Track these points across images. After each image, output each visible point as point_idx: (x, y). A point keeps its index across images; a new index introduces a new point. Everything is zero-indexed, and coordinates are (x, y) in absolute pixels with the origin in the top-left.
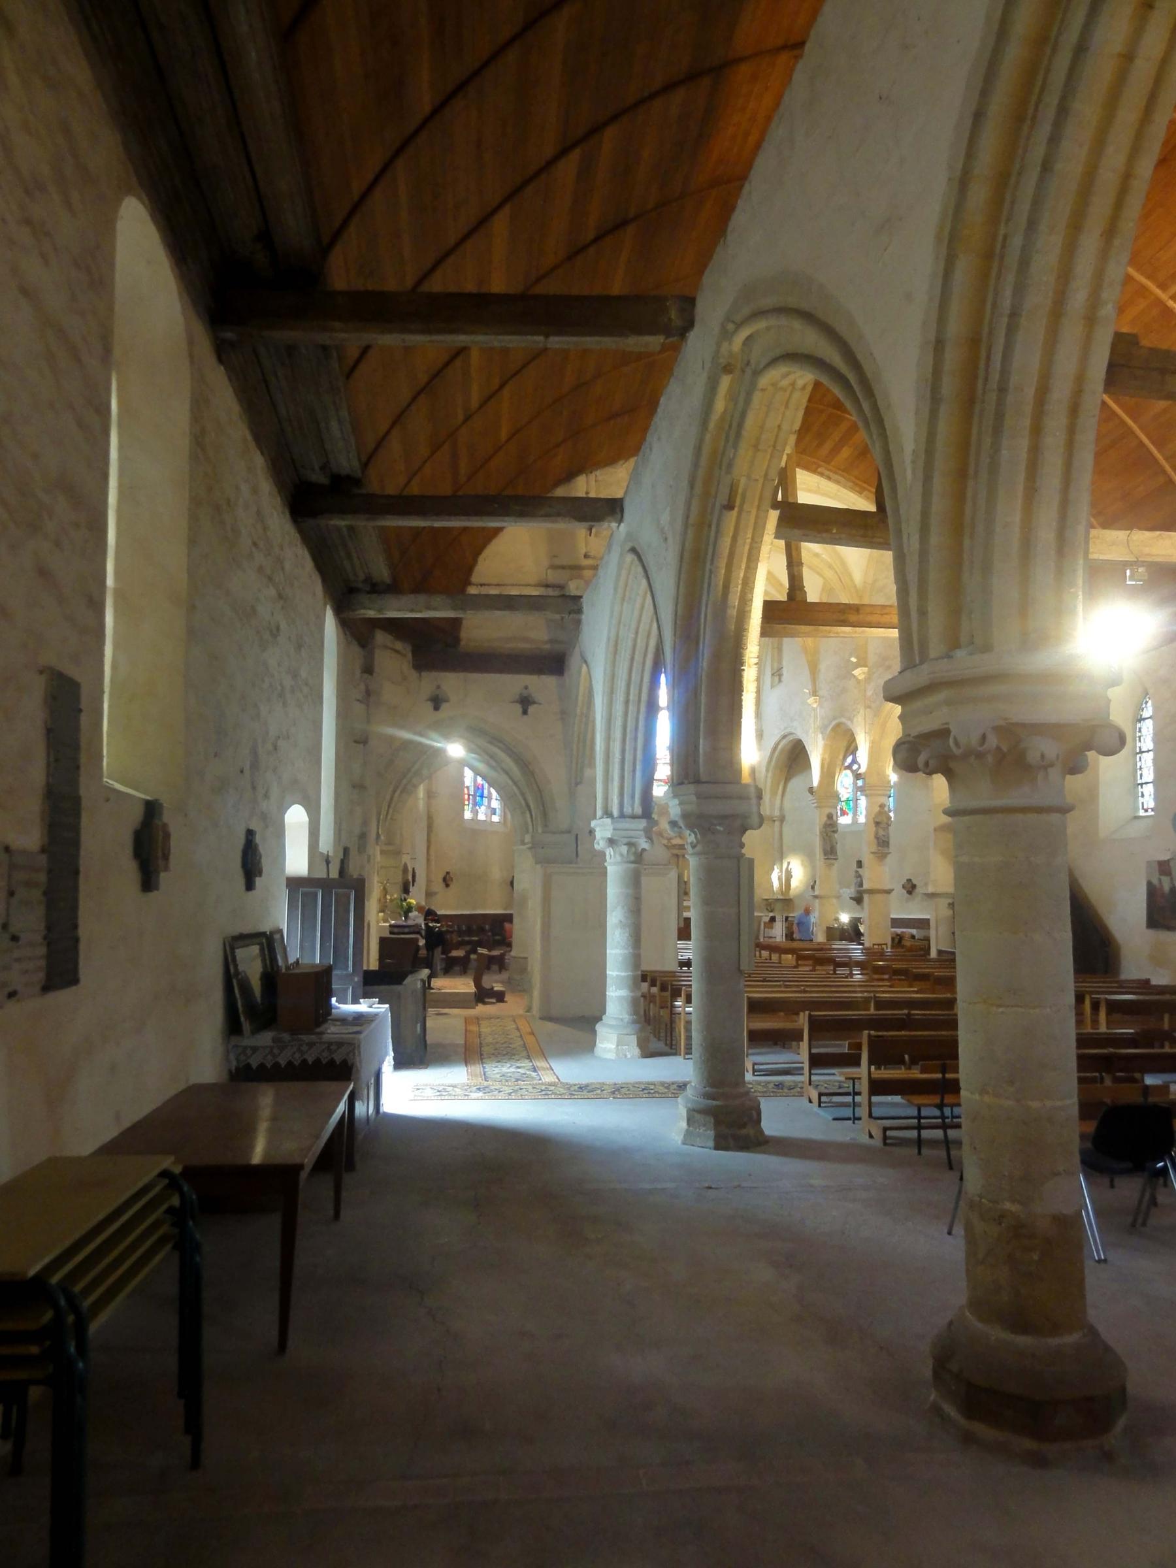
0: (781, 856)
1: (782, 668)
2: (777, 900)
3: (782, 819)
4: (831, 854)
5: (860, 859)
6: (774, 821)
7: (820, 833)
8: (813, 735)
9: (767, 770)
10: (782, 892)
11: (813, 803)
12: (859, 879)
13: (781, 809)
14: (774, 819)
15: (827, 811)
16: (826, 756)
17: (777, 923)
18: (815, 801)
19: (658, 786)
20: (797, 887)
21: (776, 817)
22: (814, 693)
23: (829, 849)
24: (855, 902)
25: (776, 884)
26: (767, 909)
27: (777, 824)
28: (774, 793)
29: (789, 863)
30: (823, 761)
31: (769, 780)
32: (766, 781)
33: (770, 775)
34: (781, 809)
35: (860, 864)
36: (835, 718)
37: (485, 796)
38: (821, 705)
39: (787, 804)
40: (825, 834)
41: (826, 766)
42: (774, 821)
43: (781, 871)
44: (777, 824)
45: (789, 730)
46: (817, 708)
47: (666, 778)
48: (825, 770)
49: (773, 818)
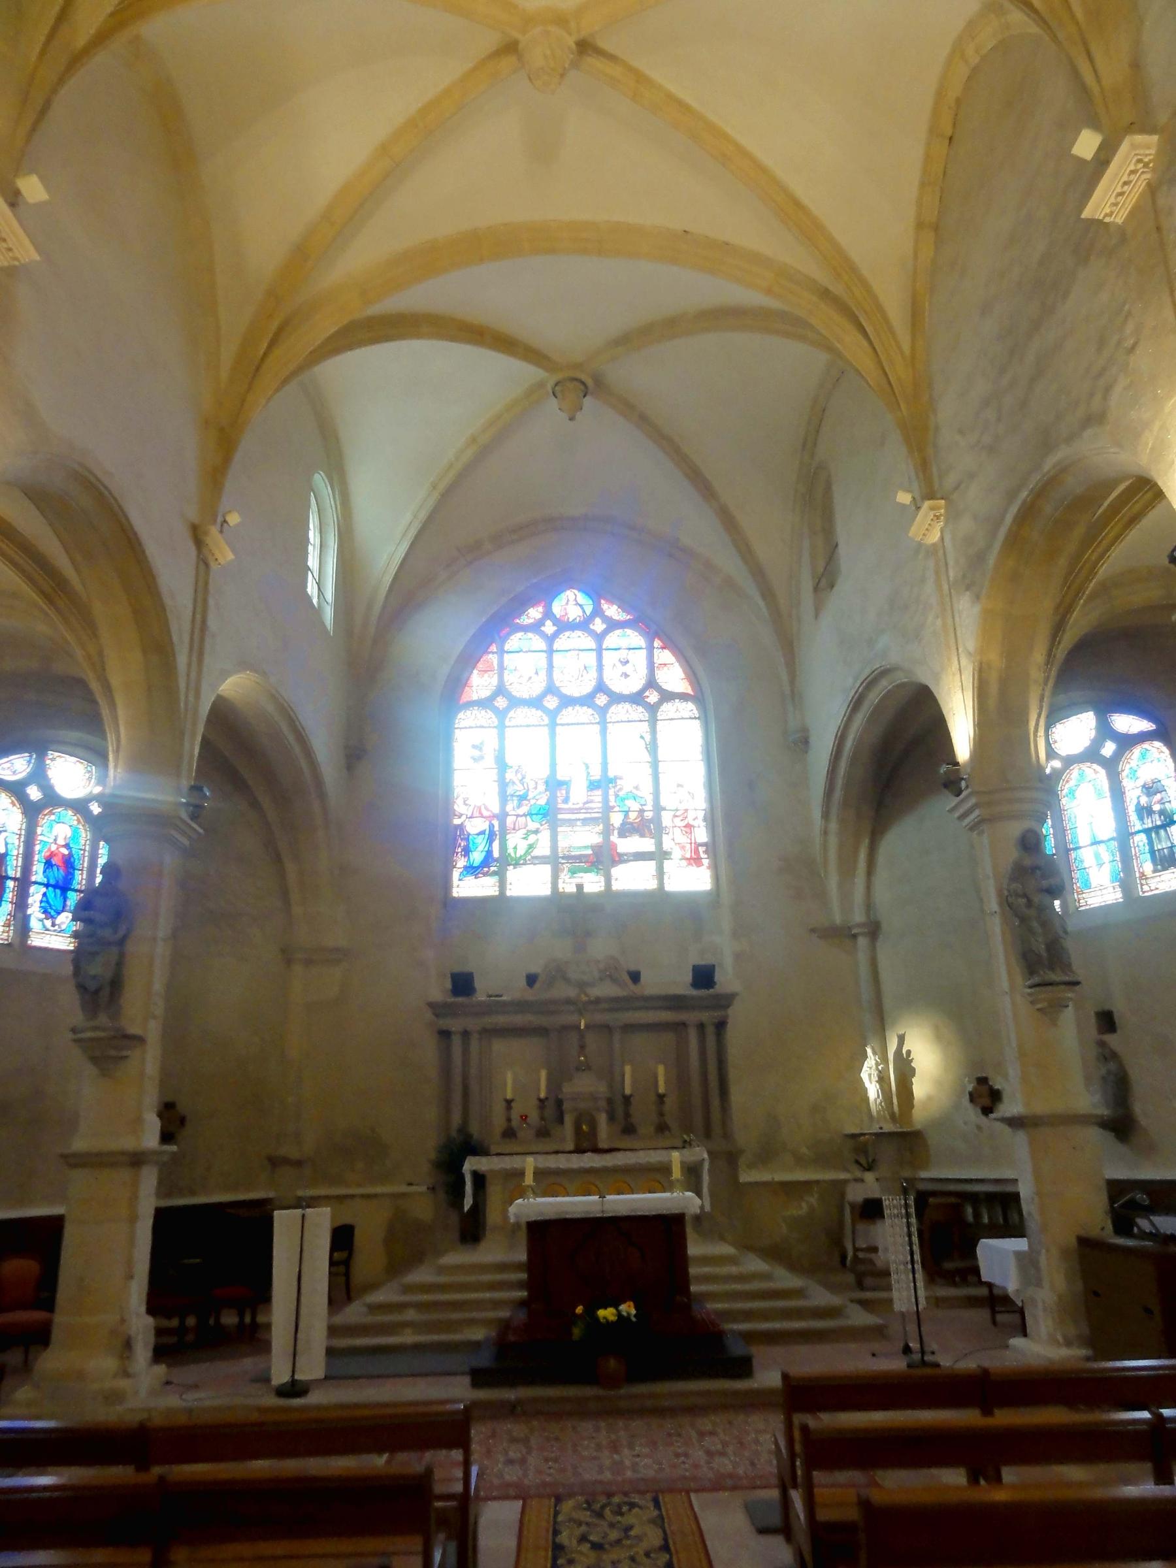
0: (880, 1022)
1: (837, 545)
2: (880, 1136)
3: (874, 930)
4: (1052, 968)
5: (1107, 1007)
6: (855, 936)
7: (1007, 902)
8: (939, 622)
9: (826, 815)
10: (893, 1116)
11: (962, 817)
12: (1112, 1066)
13: (869, 906)
14: (854, 931)
15: (1015, 829)
16: (994, 657)
17: (888, 1221)
18: (973, 801)
19: (573, 872)
20: (930, 1098)
21: (859, 925)
22: (931, 495)
23: (1044, 954)
24: (1109, 1136)
25: (873, 1090)
26: (857, 1162)
27: (862, 942)
28: (847, 869)
29: (901, 1039)
30: (981, 671)
31: (833, 841)
32: (825, 848)
33: (833, 826)
34: (869, 906)
35: (1107, 1021)
36: (1011, 495)
37: (75, 885)
38: (953, 515)
39: (883, 895)
40: (1022, 901)
41: (994, 689)
42: (855, 936)
43: (885, 1059)
44: (862, 942)
45: (867, 672)
46: (942, 538)
47: (590, 852)
48: (992, 702)
49: (850, 928)
